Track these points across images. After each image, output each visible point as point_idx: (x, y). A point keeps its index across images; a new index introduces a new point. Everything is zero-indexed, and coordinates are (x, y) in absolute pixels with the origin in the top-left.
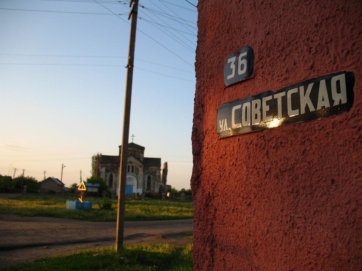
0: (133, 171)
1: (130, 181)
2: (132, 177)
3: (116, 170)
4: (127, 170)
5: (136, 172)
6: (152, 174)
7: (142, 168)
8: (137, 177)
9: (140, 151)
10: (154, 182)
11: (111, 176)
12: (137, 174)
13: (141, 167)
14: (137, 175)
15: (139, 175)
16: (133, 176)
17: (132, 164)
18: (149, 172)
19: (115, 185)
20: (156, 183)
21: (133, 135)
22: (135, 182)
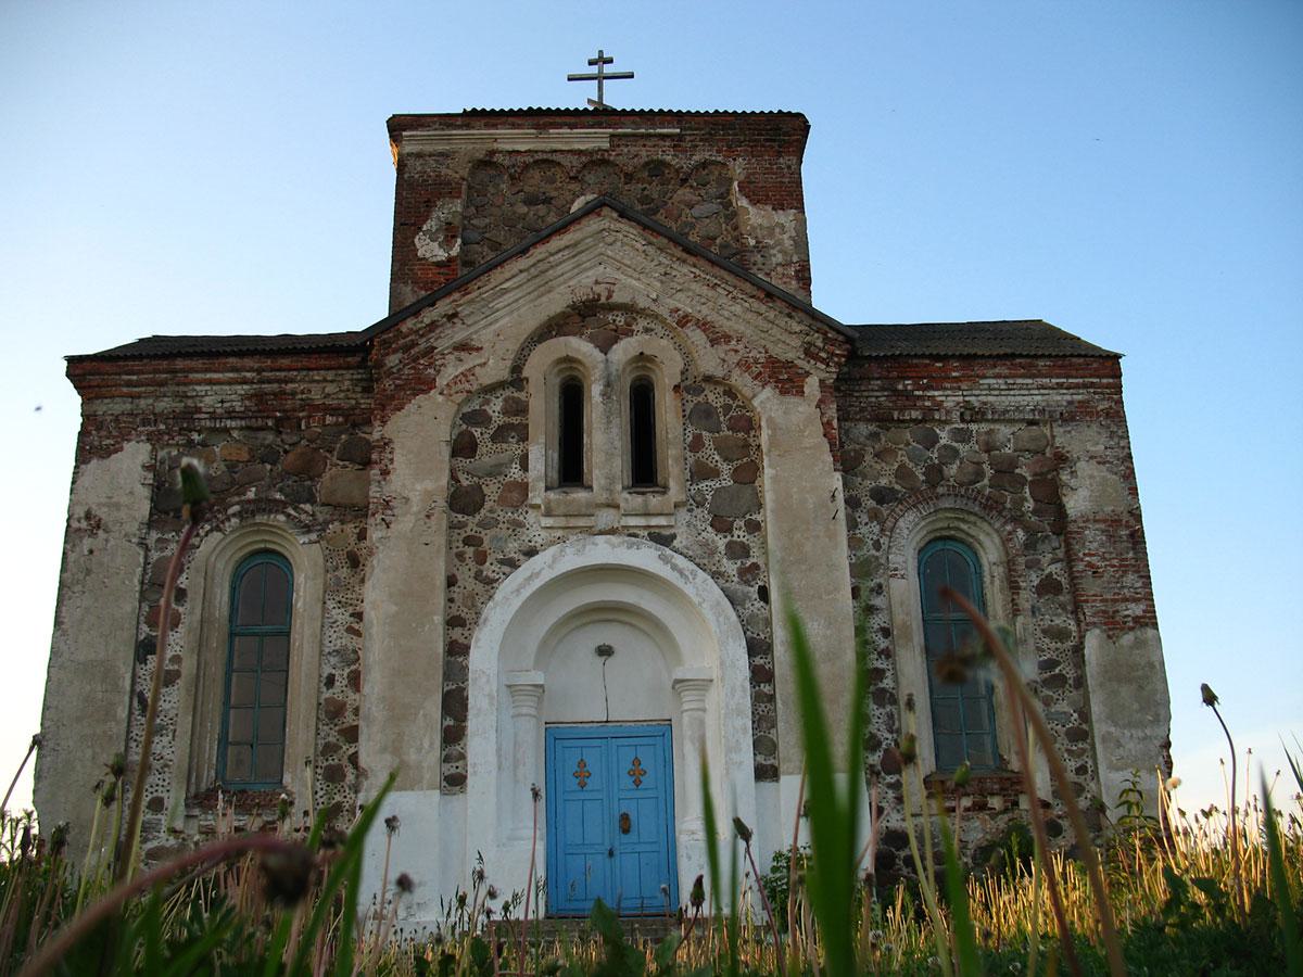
0: (644, 472)
1: (605, 651)
2: (645, 557)
3: (335, 477)
4: (541, 457)
5: (701, 472)
6: (992, 507)
7: (812, 386)
8: (731, 567)
9: (738, 168)
10: (1060, 635)
13: (785, 379)
14: (721, 525)
15: (768, 516)
16: (662, 539)
17: (623, 351)
18: (935, 474)
20: (1093, 642)
21: (603, 60)
22: (712, 650)
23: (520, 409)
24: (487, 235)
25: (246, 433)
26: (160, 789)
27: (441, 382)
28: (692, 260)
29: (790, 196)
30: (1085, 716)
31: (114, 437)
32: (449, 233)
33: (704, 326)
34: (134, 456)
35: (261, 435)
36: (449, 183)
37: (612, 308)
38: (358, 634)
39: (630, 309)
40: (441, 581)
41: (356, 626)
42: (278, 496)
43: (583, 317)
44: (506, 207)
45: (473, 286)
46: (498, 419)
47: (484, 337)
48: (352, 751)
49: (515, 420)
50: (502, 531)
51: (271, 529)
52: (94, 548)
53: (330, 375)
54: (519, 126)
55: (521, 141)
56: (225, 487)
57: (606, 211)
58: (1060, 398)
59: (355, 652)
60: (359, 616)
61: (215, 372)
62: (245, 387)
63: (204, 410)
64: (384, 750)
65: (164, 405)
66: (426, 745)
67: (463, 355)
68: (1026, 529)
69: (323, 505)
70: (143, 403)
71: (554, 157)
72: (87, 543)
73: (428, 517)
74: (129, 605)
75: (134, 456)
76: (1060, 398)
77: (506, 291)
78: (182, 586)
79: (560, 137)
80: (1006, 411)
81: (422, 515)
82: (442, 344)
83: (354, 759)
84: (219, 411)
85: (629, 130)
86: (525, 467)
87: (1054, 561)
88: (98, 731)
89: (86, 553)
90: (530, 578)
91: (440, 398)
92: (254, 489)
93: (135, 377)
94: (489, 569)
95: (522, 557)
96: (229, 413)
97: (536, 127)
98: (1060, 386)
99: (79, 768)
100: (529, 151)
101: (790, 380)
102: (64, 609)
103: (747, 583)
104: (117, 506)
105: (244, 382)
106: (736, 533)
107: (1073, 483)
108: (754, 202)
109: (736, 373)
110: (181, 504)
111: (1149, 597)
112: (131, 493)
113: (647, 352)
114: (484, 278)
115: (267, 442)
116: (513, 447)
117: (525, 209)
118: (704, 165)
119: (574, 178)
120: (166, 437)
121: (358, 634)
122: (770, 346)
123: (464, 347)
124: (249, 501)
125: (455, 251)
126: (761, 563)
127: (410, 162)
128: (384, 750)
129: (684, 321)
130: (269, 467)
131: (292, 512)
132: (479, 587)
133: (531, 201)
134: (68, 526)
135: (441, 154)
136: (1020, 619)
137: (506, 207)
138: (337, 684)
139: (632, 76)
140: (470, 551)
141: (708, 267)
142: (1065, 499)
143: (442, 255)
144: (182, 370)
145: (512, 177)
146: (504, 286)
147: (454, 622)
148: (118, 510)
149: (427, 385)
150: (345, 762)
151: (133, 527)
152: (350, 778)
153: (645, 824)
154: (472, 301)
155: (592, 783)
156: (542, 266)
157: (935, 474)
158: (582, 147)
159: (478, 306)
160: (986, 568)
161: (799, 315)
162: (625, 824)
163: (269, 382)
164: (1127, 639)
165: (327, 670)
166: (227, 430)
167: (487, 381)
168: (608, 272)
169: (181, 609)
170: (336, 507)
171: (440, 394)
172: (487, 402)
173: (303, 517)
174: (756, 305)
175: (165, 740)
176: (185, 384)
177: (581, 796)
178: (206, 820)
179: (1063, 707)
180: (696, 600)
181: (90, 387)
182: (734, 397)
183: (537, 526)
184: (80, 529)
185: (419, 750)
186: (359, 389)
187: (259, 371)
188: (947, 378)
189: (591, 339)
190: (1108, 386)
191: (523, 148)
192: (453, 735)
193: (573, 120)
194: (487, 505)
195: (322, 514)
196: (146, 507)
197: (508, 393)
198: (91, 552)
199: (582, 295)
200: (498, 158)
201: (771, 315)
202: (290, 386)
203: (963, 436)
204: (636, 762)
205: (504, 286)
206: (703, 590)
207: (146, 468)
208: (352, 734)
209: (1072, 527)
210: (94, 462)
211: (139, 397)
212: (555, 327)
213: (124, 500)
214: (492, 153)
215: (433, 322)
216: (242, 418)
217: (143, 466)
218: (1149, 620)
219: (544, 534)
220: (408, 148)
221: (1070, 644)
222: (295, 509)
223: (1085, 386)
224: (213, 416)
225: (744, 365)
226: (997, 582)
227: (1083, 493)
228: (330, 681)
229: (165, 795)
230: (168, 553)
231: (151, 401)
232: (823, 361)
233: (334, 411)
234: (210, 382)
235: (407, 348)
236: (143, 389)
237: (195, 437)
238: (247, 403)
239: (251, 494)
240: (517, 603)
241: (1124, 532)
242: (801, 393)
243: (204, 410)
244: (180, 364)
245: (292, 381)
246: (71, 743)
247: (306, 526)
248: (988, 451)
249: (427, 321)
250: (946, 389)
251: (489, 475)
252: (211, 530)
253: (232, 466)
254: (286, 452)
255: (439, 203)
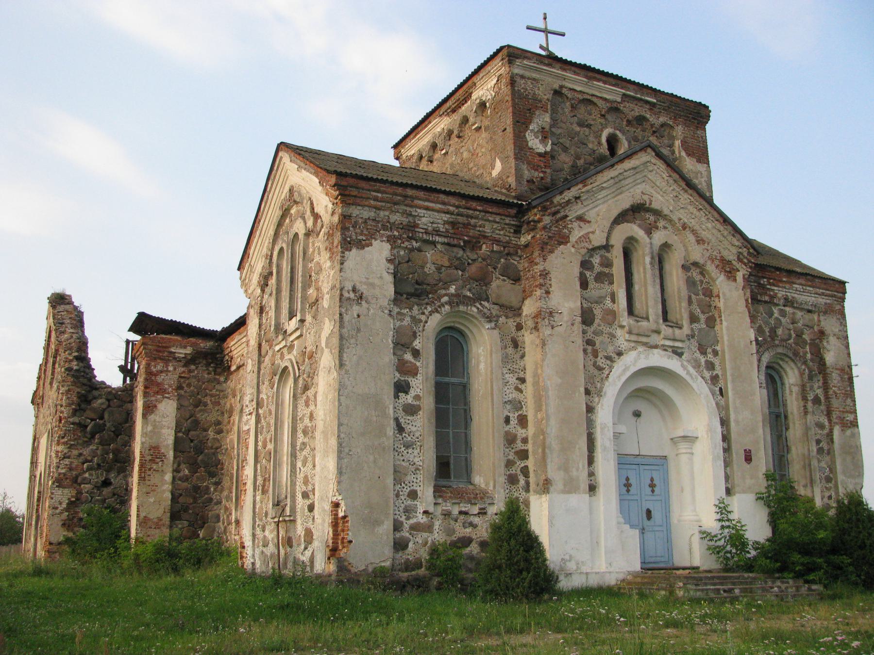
2: (673, 364)
3: (499, 286)
7: (739, 276)
8: (707, 375)
10: (821, 426)
11: (451, 349)
12: (706, 345)
16: (677, 353)
17: (659, 237)
18: (773, 331)
19: (509, 464)
23: (608, 264)
24: (561, 141)
25: (447, 247)
26: (415, 484)
27: (573, 239)
28: (690, 191)
29: (701, 154)
30: (832, 470)
31: (365, 235)
32: (544, 135)
33: (694, 232)
34: (379, 252)
35: (455, 250)
36: (540, 101)
37: (649, 210)
38: (521, 391)
39: (657, 213)
40: (581, 367)
41: (520, 386)
42: (468, 294)
43: (634, 212)
44: (568, 124)
45: (589, 181)
46: (598, 268)
47: (591, 215)
48: (522, 465)
49: (606, 270)
50: (605, 338)
51: (466, 316)
52: (361, 314)
53: (498, 219)
54: (578, 74)
55: (576, 83)
56: (435, 282)
57: (649, 150)
58: (822, 300)
59: (520, 402)
60: (523, 380)
61: (432, 202)
62: (448, 216)
63: (421, 226)
64: (559, 468)
65: (396, 218)
66: (581, 466)
67: (582, 224)
68: (809, 368)
69: (494, 304)
70: (382, 213)
71: (594, 99)
72: (356, 309)
73: (573, 325)
74: (388, 358)
75: (379, 252)
76: (822, 300)
77: (603, 188)
78: (417, 348)
79: (599, 89)
80: (802, 304)
81: (569, 323)
82: (572, 215)
83: (525, 471)
84: (430, 228)
85: (632, 94)
86: (613, 301)
87: (819, 387)
88: (376, 443)
89: (356, 316)
90: (624, 371)
91: (573, 250)
92: (454, 287)
93: (380, 195)
94: (601, 362)
95: (617, 357)
96: (437, 231)
97: (586, 77)
98: (823, 294)
99: (366, 468)
100: (581, 92)
101: (730, 272)
102: (345, 355)
103: (714, 384)
104: (372, 285)
105: (447, 213)
106: (709, 356)
107: (828, 347)
108: (689, 155)
109: (709, 262)
110: (411, 289)
111: (855, 412)
112: (381, 277)
113: (669, 242)
114: (594, 178)
115: (459, 256)
116: (606, 289)
117: (578, 129)
118: (663, 125)
119: (603, 116)
120: (399, 241)
121: (521, 391)
122: (722, 250)
123: (580, 218)
124: (452, 295)
125: (549, 148)
126: (720, 374)
127: (518, 79)
128: (559, 468)
129: (684, 227)
130: (460, 273)
131: (479, 306)
132: (596, 372)
133: (581, 124)
134: (341, 295)
135: (534, 79)
136: (809, 417)
137: (568, 124)
138: (511, 422)
139: (563, 35)
140: (590, 348)
141: (697, 197)
142: (825, 356)
143: (541, 149)
144: (411, 197)
145: (572, 106)
146: (604, 185)
147: (587, 392)
148: (374, 288)
149: (564, 240)
150: (519, 472)
151: (385, 302)
152: (522, 482)
153: (657, 515)
154: (588, 191)
155: (633, 490)
156: (621, 177)
157: (773, 331)
158: (608, 97)
159: (590, 194)
160: (787, 386)
161: (738, 236)
162: (649, 513)
163: (462, 215)
164: (848, 432)
165: (506, 413)
166: (434, 243)
167: (597, 244)
168: (647, 188)
169: (418, 364)
170: (501, 306)
171: (573, 246)
172: (592, 256)
173: (485, 310)
174: (718, 226)
175: (416, 452)
176: (411, 206)
177: (629, 497)
178: (446, 506)
179: (823, 464)
180: (698, 392)
181: (349, 195)
182: (704, 277)
183: (622, 338)
184: (349, 299)
185: (577, 470)
186: (512, 231)
187: (457, 207)
188: (781, 281)
189: (640, 226)
190: (840, 298)
191: (578, 88)
192: (591, 461)
193: (604, 78)
194: (597, 321)
195: (495, 310)
196: (390, 290)
197: (603, 252)
198: (359, 316)
199: (638, 199)
200: (564, 91)
201: (726, 233)
202: (473, 221)
203: (783, 313)
204: (652, 480)
205: (604, 185)
206: (700, 386)
207: (390, 261)
208: (523, 455)
209: (828, 371)
210: (354, 250)
211: (379, 209)
212: (622, 218)
213: (377, 282)
214: (561, 87)
215: (569, 200)
216: (445, 237)
217: (387, 260)
218: (854, 424)
219: (626, 343)
220: (516, 71)
221: (826, 431)
222: (481, 304)
223: (832, 296)
224: (427, 232)
225: (712, 260)
226: (794, 395)
227: (832, 353)
228: (507, 420)
229: (418, 489)
230: (405, 323)
231: (387, 213)
232: (745, 264)
233: (498, 242)
234: (427, 208)
235: (554, 214)
236: (383, 204)
237: (414, 243)
238: (447, 226)
239: (452, 289)
240: (619, 384)
241: (846, 376)
242: (735, 280)
243: (421, 226)
244: (410, 192)
245: (476, 218)
246: (359, 450)
247: (488, 317)
248: (792, 324)
249: (567, 199)
250: (779, 286)
251: (597, 302)
252: (431, 313)
253: (439, 269)
254: (469, 264)
255: (537, 113)
